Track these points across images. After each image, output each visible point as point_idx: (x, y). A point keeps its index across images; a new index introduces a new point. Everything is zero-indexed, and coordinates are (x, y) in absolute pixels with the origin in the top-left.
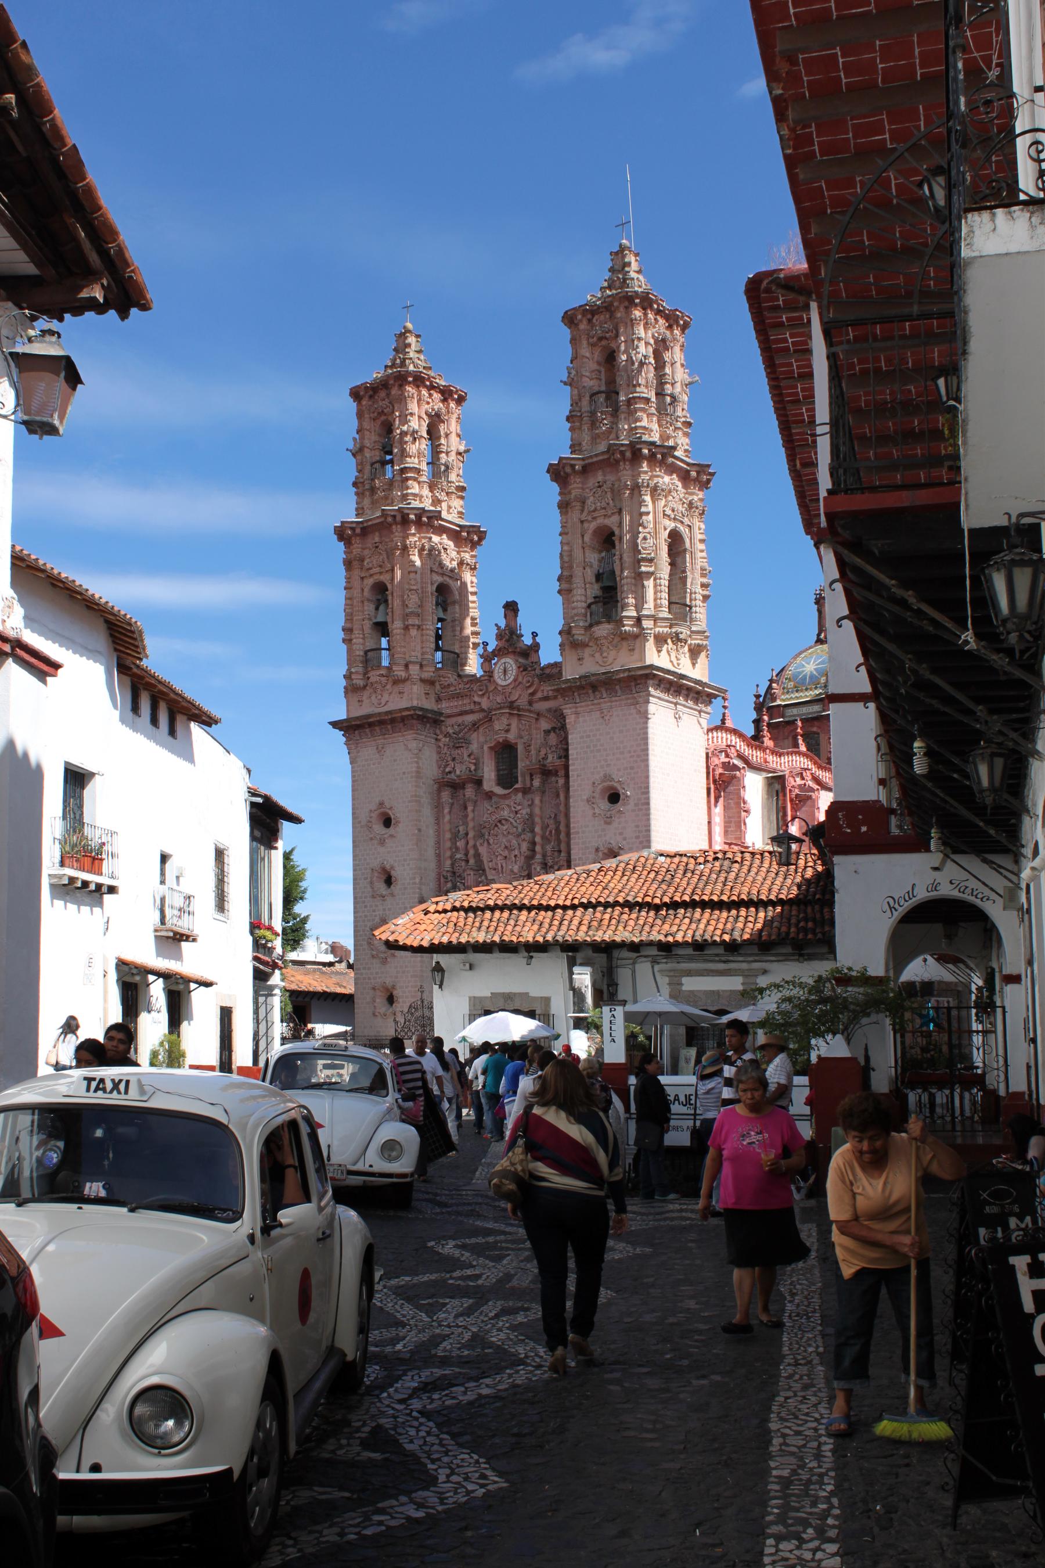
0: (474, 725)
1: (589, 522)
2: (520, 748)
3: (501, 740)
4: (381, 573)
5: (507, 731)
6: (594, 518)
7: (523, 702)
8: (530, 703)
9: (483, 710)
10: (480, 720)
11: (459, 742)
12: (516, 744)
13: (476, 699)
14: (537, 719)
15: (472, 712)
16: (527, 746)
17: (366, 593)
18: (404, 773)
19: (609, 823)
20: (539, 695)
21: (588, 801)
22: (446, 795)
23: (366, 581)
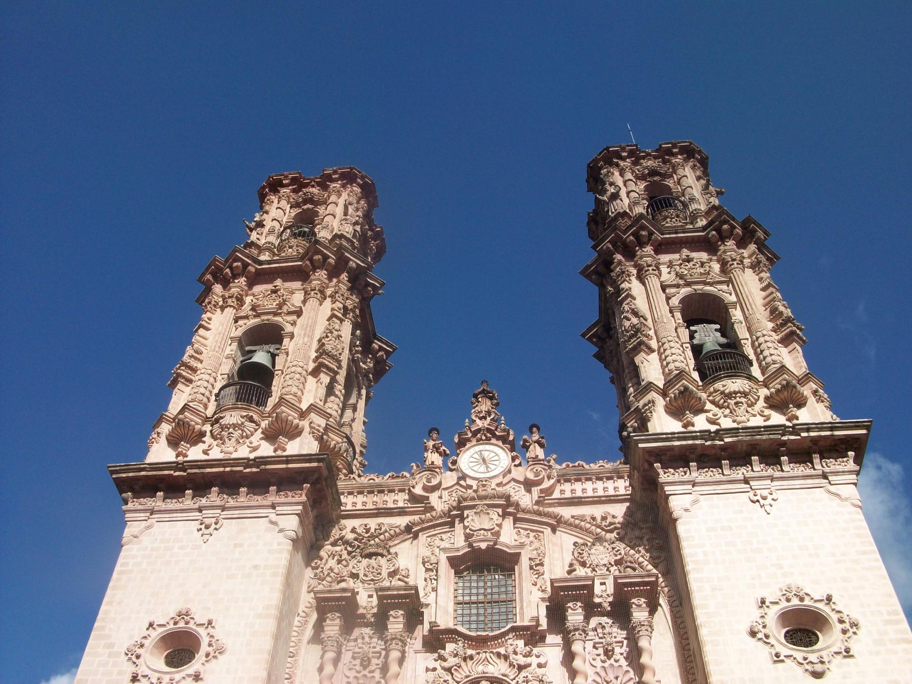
0: (408, 529)
1: (678, 286)
2: (524, 562)
3: (483, 546)
4: (275, 314)
5: (498, 534)
6: (688, 284)
7: (526, 500)
8: (538, 503)
9: (432, 509)
10: (423, 521)
11: (369, 548)
12: (515, 558)
13: (418, 491)
14: (554, 531)
15: (402, 512)
16: (537, 566)
17: (239, 333)
18: (256, 567)
19: (817, 675)
20: (556, 495)
21: (753, 634)
22: (333, 627)
23: (241, 322)
